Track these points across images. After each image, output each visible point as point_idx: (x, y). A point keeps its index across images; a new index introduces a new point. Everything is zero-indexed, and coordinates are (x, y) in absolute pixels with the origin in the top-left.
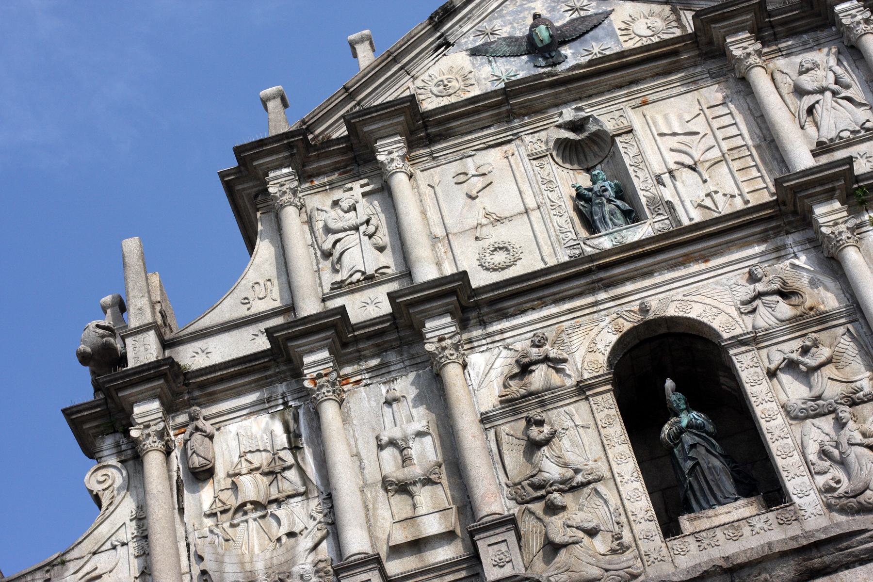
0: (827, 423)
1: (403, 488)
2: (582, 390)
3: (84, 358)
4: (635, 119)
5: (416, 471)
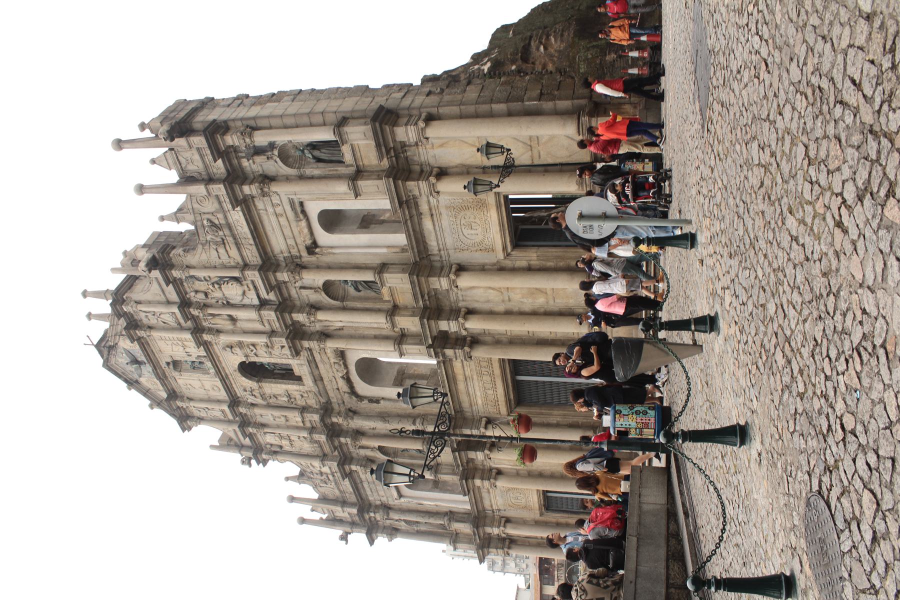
0: (273, 352)
3: (250, 465)
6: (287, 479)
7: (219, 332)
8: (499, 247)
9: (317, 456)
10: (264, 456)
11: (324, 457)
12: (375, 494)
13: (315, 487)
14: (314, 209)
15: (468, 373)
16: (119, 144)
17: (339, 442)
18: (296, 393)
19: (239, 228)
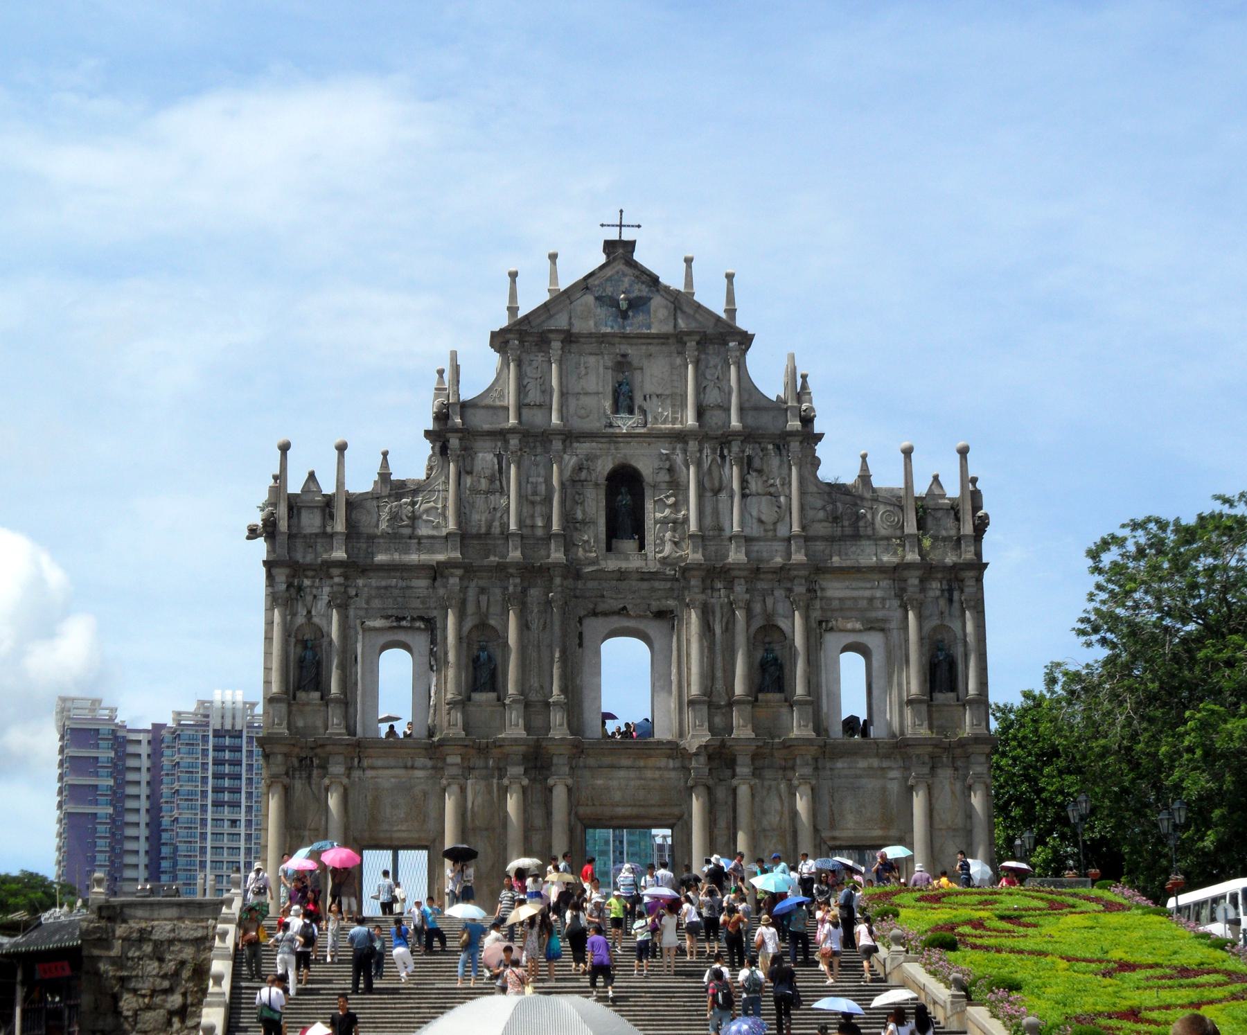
1: (533, 503)
2: (597, 485)
4: (645, 363)
5: (538, 498)
6: (385, 454)
7: (699, 465)
8: (837, 834)
9: (459, 523)
10: (454, 442)
11: (464, 537)
12: (373, 592)
13: (374, 496)
14: (874, 641)
15: (649, 774)
16: (963, 452)
17: (512, 575)
18: (592, 535)
19: (854, 548)
